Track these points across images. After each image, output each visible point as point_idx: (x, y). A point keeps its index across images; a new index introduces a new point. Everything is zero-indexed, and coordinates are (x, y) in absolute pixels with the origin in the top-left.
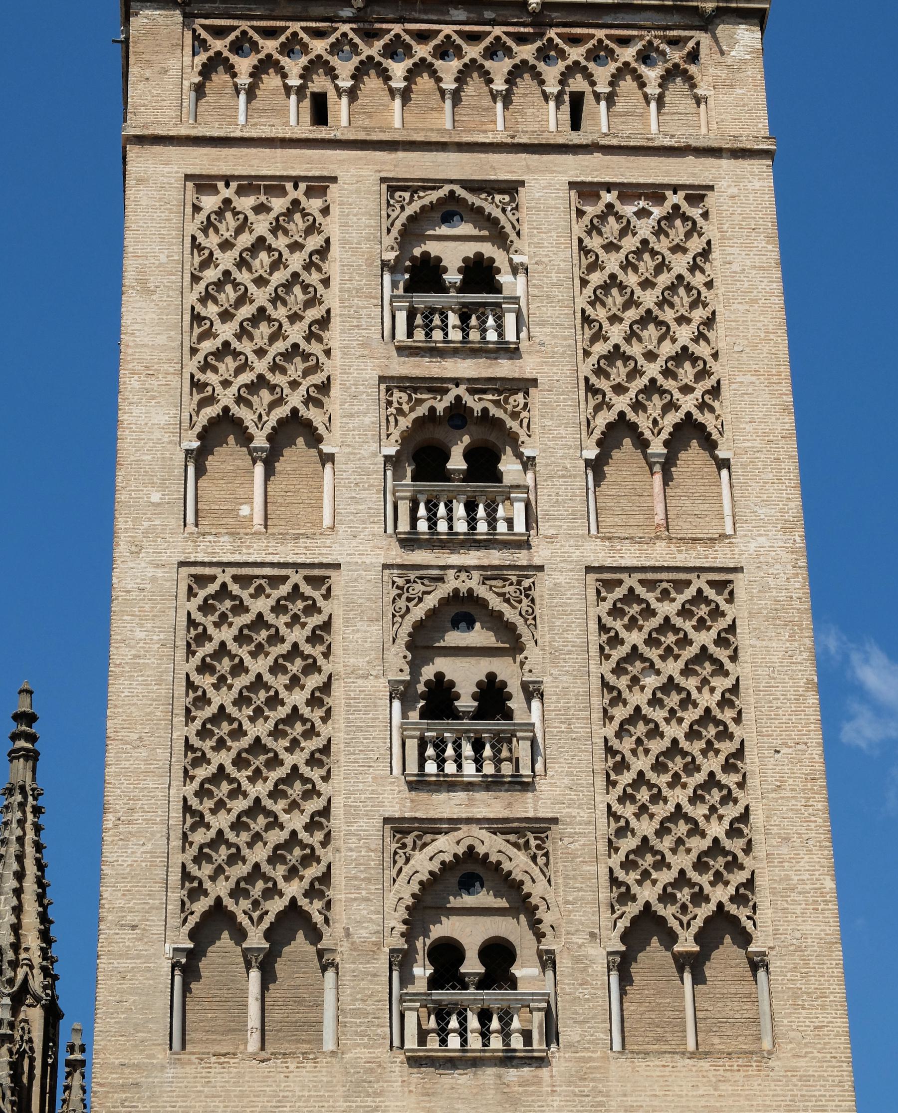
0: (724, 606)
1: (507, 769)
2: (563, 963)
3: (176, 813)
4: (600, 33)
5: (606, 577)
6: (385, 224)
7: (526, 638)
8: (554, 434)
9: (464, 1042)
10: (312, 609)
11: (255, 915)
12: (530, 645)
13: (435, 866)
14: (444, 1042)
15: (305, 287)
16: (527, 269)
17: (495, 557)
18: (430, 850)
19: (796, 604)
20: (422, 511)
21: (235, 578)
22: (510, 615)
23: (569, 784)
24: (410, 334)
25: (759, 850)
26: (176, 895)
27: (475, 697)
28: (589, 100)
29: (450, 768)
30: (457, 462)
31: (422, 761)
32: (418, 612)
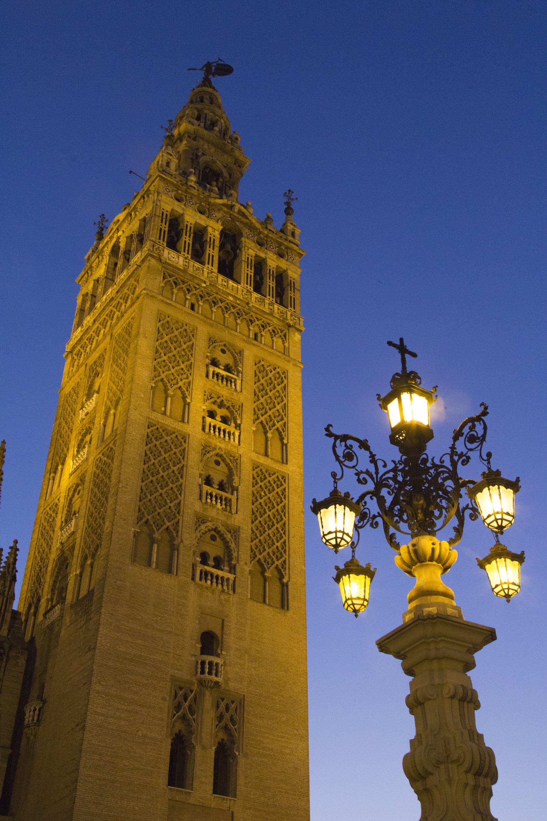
0: (283, 483)
3: (139, 491)
4: (264, 319)
6: (208, 345)
11: (158, 528)
12: (235, 475)
13: (207, 529)
14: (206, 582)
16: (242, 373)
17: (229, 448)
18: (206, 525)
19: (300, 488)
20: (212, 429)
22: (231, 465)
23: (242, 518)
24: (213, 378)
26: (137, 514)
27: (218, 485)
28: (259, 335)
30: (218, 418)
31: (206, 499)
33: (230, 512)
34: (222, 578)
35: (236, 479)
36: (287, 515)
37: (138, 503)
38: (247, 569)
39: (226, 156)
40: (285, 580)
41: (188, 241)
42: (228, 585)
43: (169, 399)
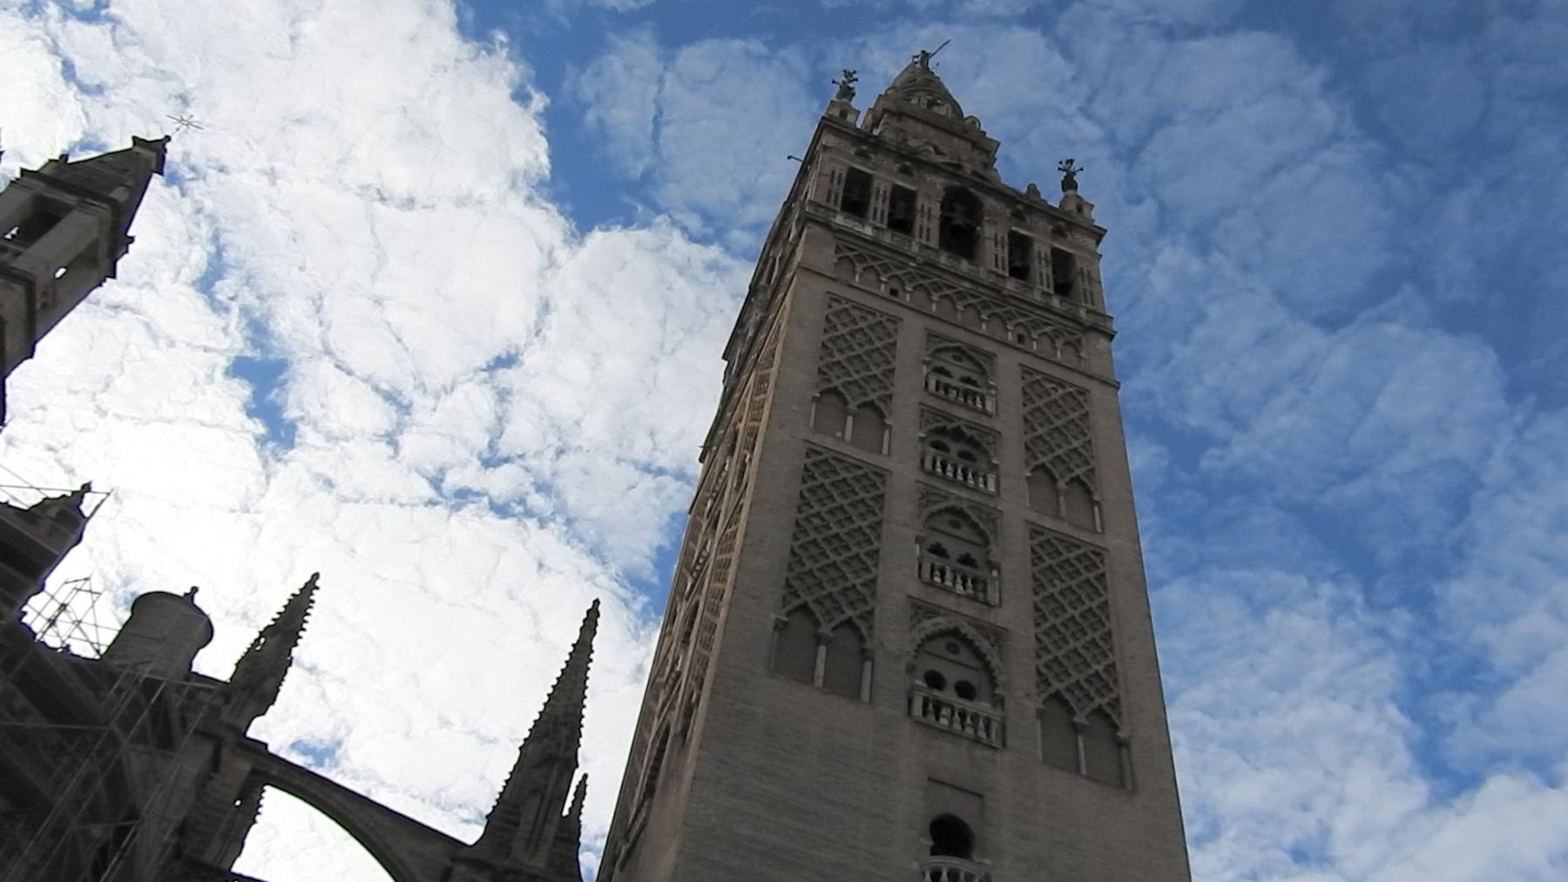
1: (981, 595)
2: (1010, 704)
3: (787, 553)
5: (1036, 531)
7: (991, 539)
8: (1011, 457)
9: (951, 722)
10: (875, 486)
13: (935, 629)
14: (937, 718)
15: (882, 355)
17: (977, 498)
21: (835, 459)
22: (982, 526)
25: (1121, 684)
28: (1027, 341)
29: (948, 583)
32: (934, 508)
33: (986, 603)
34: (975, 717)
35: (994, 549)
36: (1113, 618)
37: (785, 574)
38: (1032, 706)
39: (955, 140)
40: (1122, 734)
41: (880, 206)
42: (987, 729)
43: (850, 419)
